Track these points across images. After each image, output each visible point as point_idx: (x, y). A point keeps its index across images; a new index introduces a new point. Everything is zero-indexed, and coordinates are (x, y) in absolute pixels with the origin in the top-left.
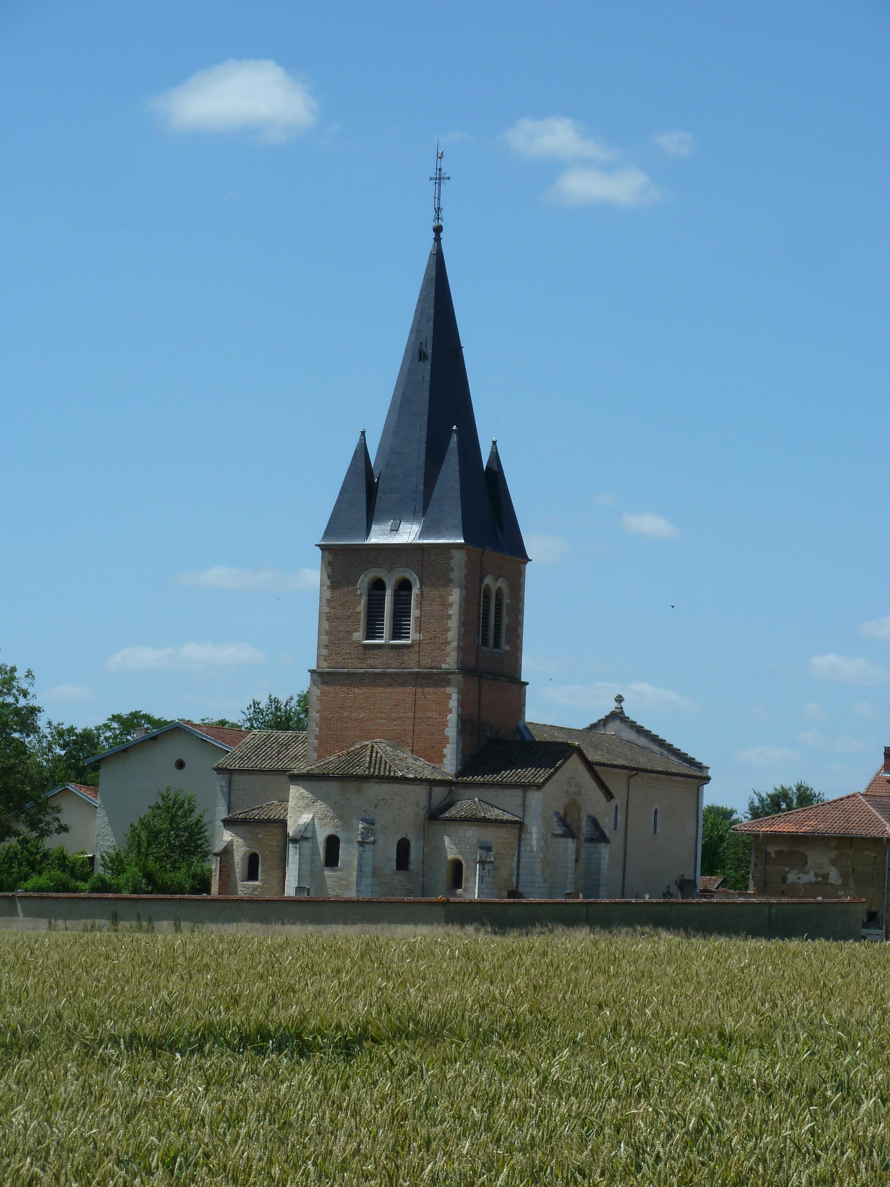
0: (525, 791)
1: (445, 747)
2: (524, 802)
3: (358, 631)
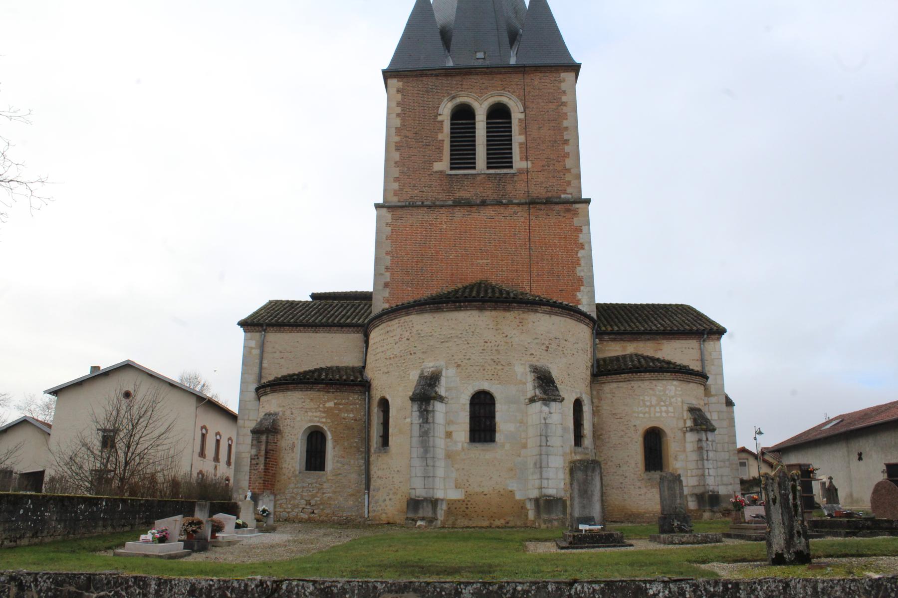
1: (578, 290)
2: (702, 354)
3: (441, 160)
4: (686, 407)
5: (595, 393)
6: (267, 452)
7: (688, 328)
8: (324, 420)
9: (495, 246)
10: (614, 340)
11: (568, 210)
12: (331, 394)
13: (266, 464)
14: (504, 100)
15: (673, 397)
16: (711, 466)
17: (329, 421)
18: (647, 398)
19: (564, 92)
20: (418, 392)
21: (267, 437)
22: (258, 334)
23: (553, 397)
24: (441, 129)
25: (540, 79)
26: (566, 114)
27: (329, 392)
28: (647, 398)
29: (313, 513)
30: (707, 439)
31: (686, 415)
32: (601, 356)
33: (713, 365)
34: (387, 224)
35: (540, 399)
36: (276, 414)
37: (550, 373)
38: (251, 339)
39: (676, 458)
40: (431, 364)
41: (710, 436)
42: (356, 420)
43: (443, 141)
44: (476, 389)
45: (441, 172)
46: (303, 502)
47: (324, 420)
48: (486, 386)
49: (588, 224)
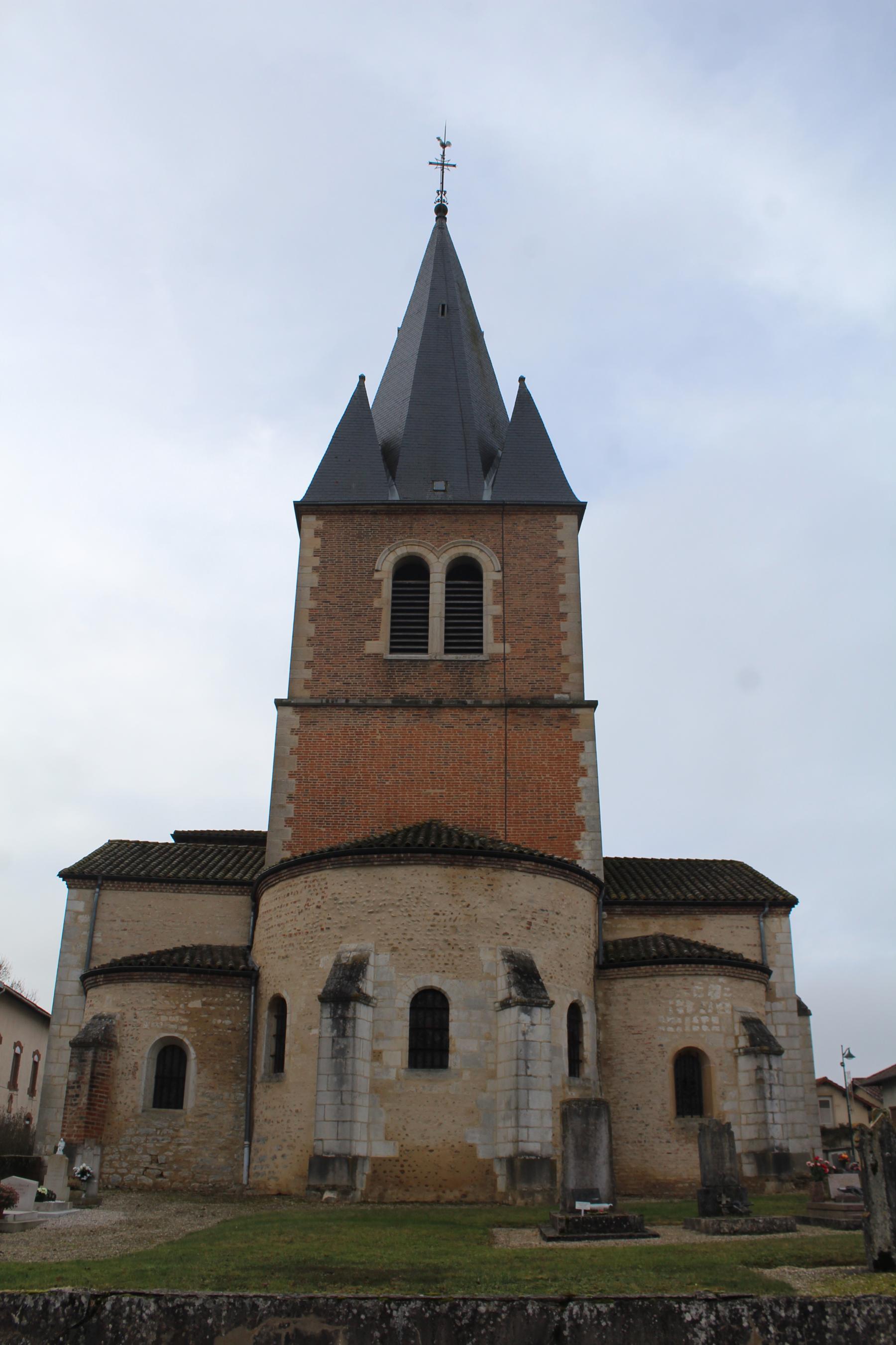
2: (762, 936)
3: (377, 638)
4: (737, 1017)
5: (600, 994)
6: (93, 1077)
7: (740, 896)
8: (185, 1028)
9: (454, 768)
10: (630, 913)
11: (563, 718)
12: (198, 988)
13: (91, 1097)
14: (473, 552)
15: (718, 1001)
16: (776, 1109)
17: (193, 1030)
18: (679, 1003)
19: (561, 543)
20: (331, 988)
21: (95, 1053)
22: (89, 892)
23: (537, 1001)
24: (378, 592)
25: (527, 522)
26: (563, 575)
27: (194, 985)
28: (679, 1003)
29: (161, 1175)
30: (770, 1067)
31: (738, 1029)
32: (610, 937)
33: (778, 953)
34: (293, 730)
35: (517, 1003)
36: (111, 1017)
37: (532, 962)
38: (78, 899)
39: (723, 1096)
40: (353, 946)
41: (775, 1062)
42: (234, 1029)
43: (381, 609)
44: (421, 985)
45: (376, 655)
46: (147, 1158)
47: (185, 1028)
48: (435, 981)
49: (593, 739)
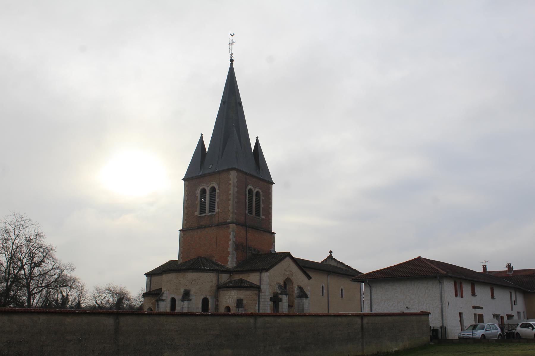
0: (261, 273)
2: (260, 278)
11: (227, 227)
48: (173, 296)
